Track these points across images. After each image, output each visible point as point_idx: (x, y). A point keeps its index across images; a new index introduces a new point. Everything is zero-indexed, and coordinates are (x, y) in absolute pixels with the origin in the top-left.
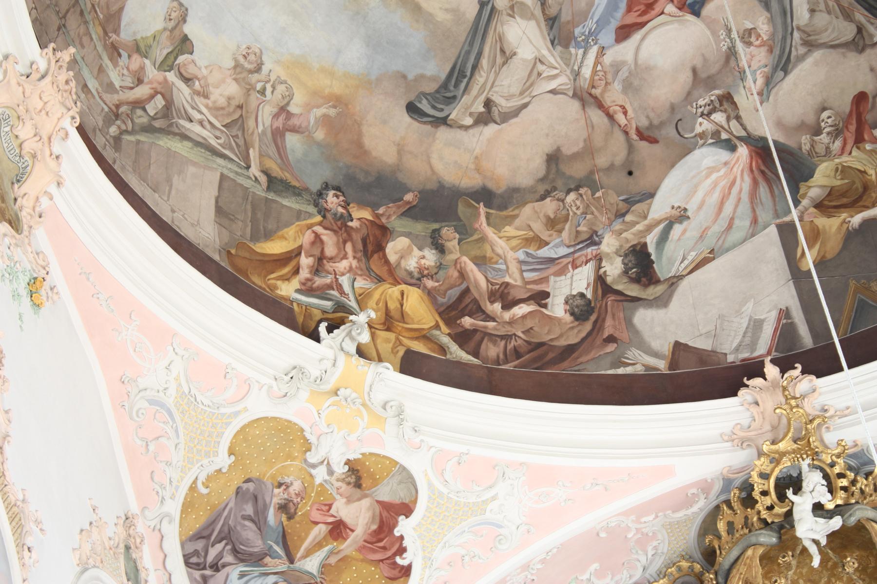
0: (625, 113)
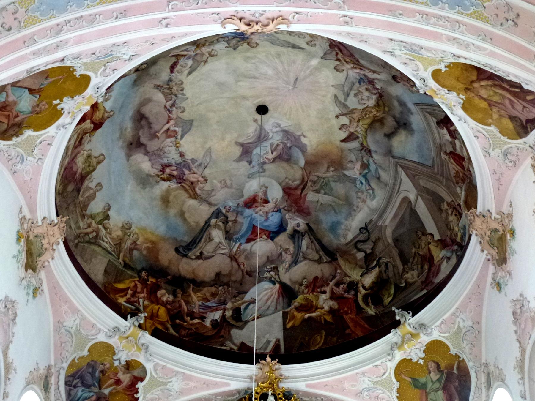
0: (244, 265)
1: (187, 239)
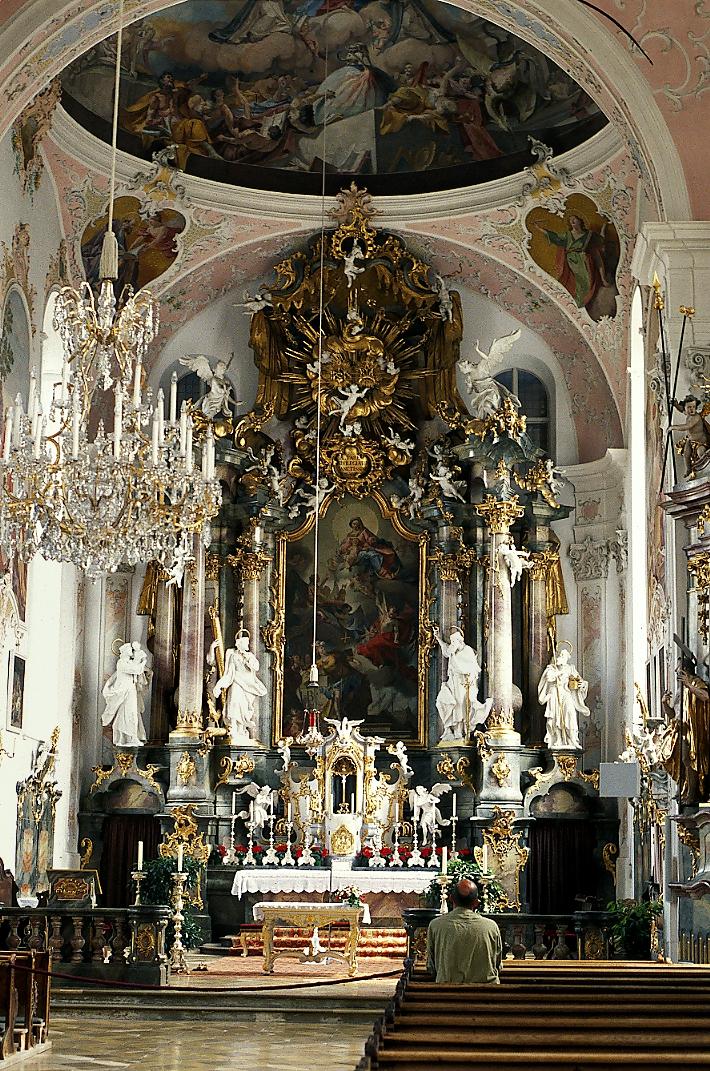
1: (227, 19)
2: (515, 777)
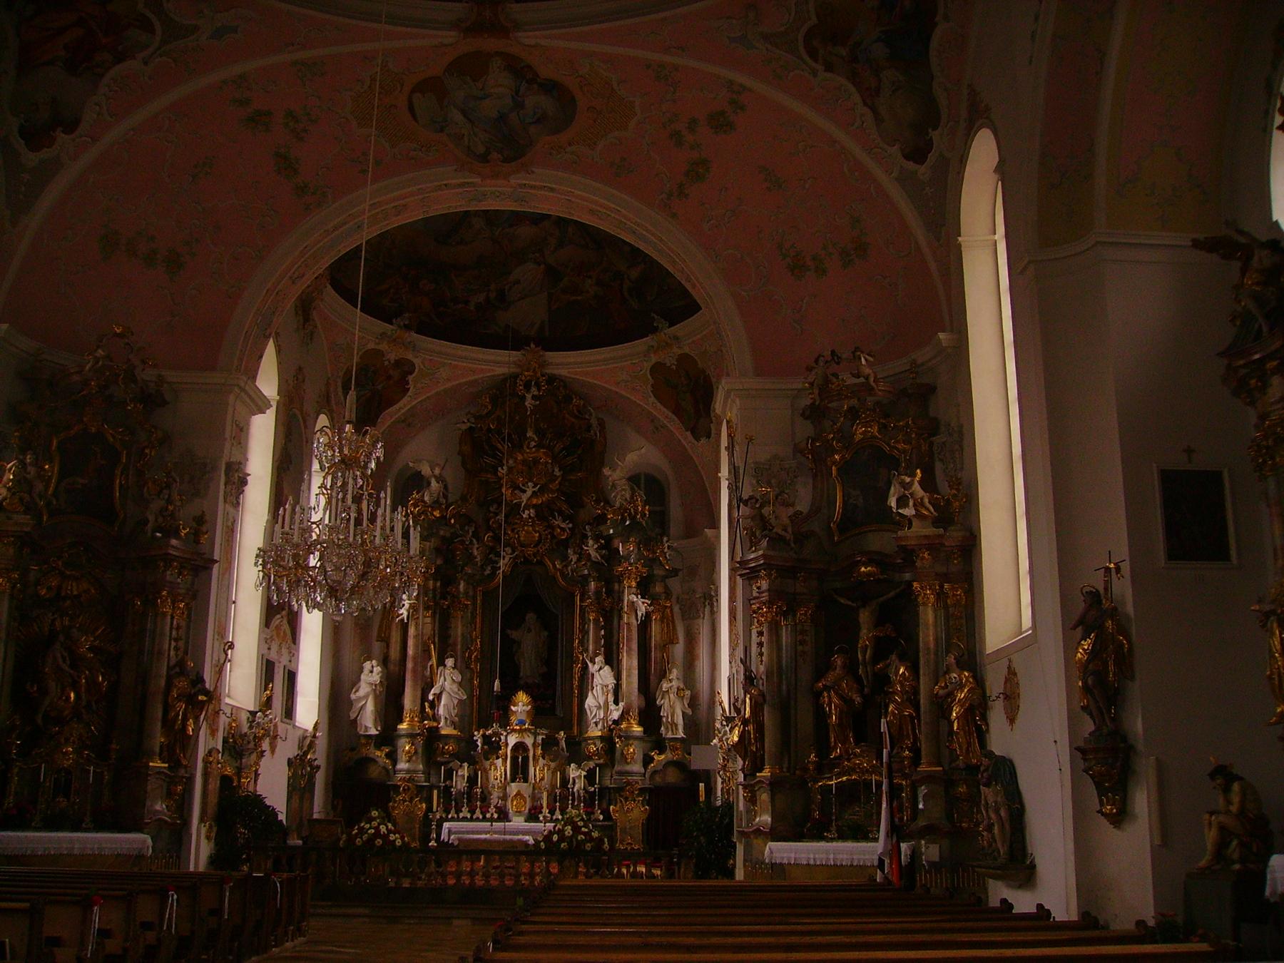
2: (639, 756)
